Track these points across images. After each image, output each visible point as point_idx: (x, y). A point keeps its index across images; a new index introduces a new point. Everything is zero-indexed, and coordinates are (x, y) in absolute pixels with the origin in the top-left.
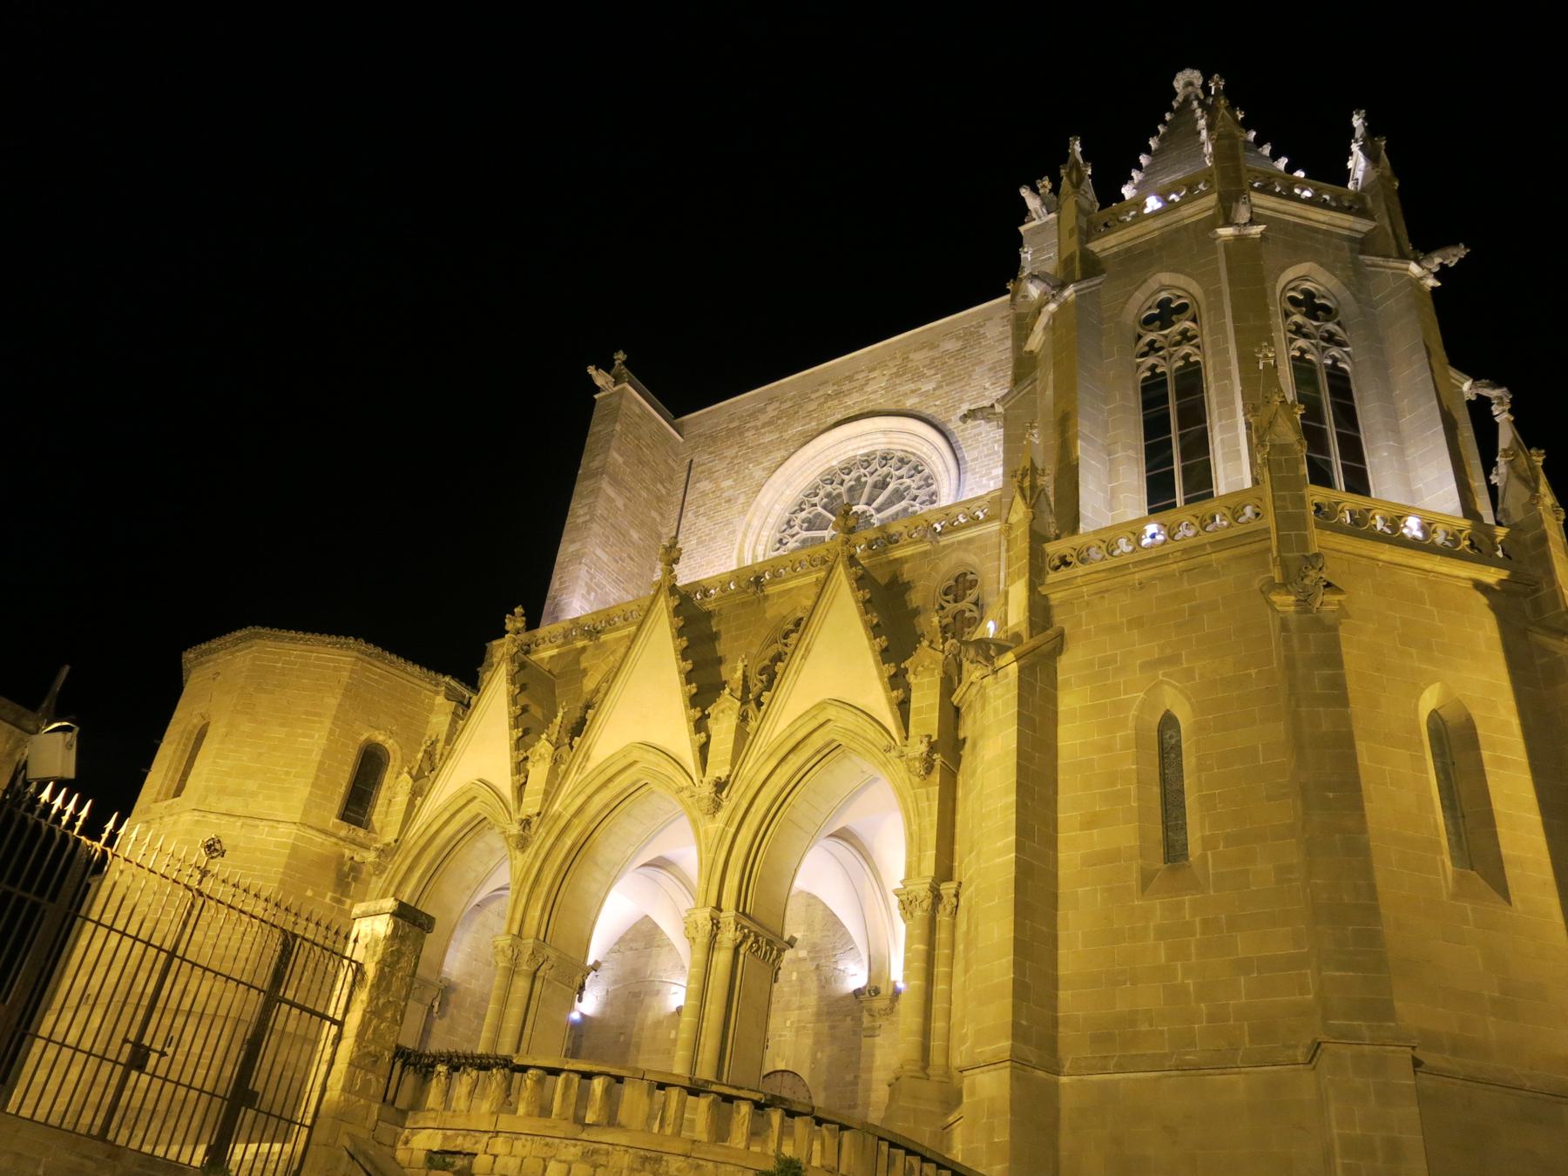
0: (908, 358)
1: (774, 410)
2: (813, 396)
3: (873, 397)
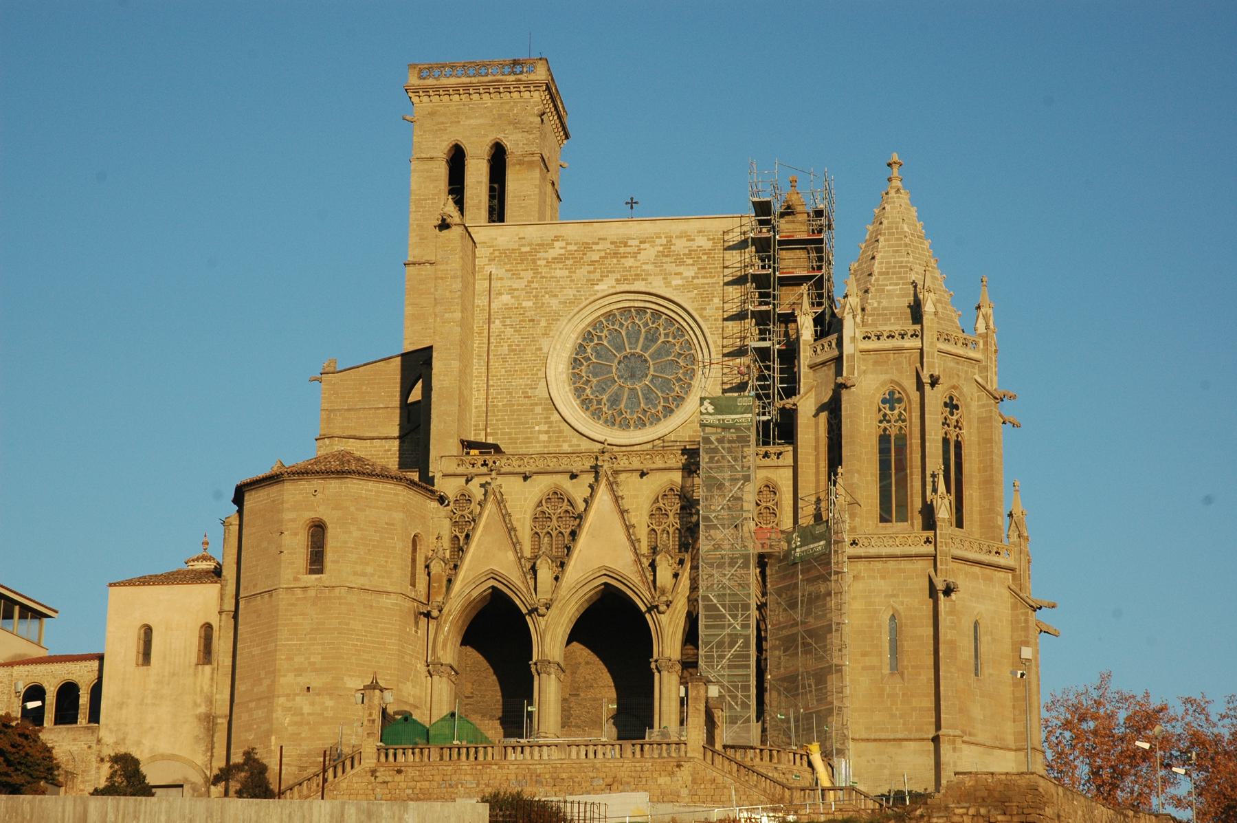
0: (671, 241)
1: (561, 248)
2: (595, 247)
3: (645, 267)
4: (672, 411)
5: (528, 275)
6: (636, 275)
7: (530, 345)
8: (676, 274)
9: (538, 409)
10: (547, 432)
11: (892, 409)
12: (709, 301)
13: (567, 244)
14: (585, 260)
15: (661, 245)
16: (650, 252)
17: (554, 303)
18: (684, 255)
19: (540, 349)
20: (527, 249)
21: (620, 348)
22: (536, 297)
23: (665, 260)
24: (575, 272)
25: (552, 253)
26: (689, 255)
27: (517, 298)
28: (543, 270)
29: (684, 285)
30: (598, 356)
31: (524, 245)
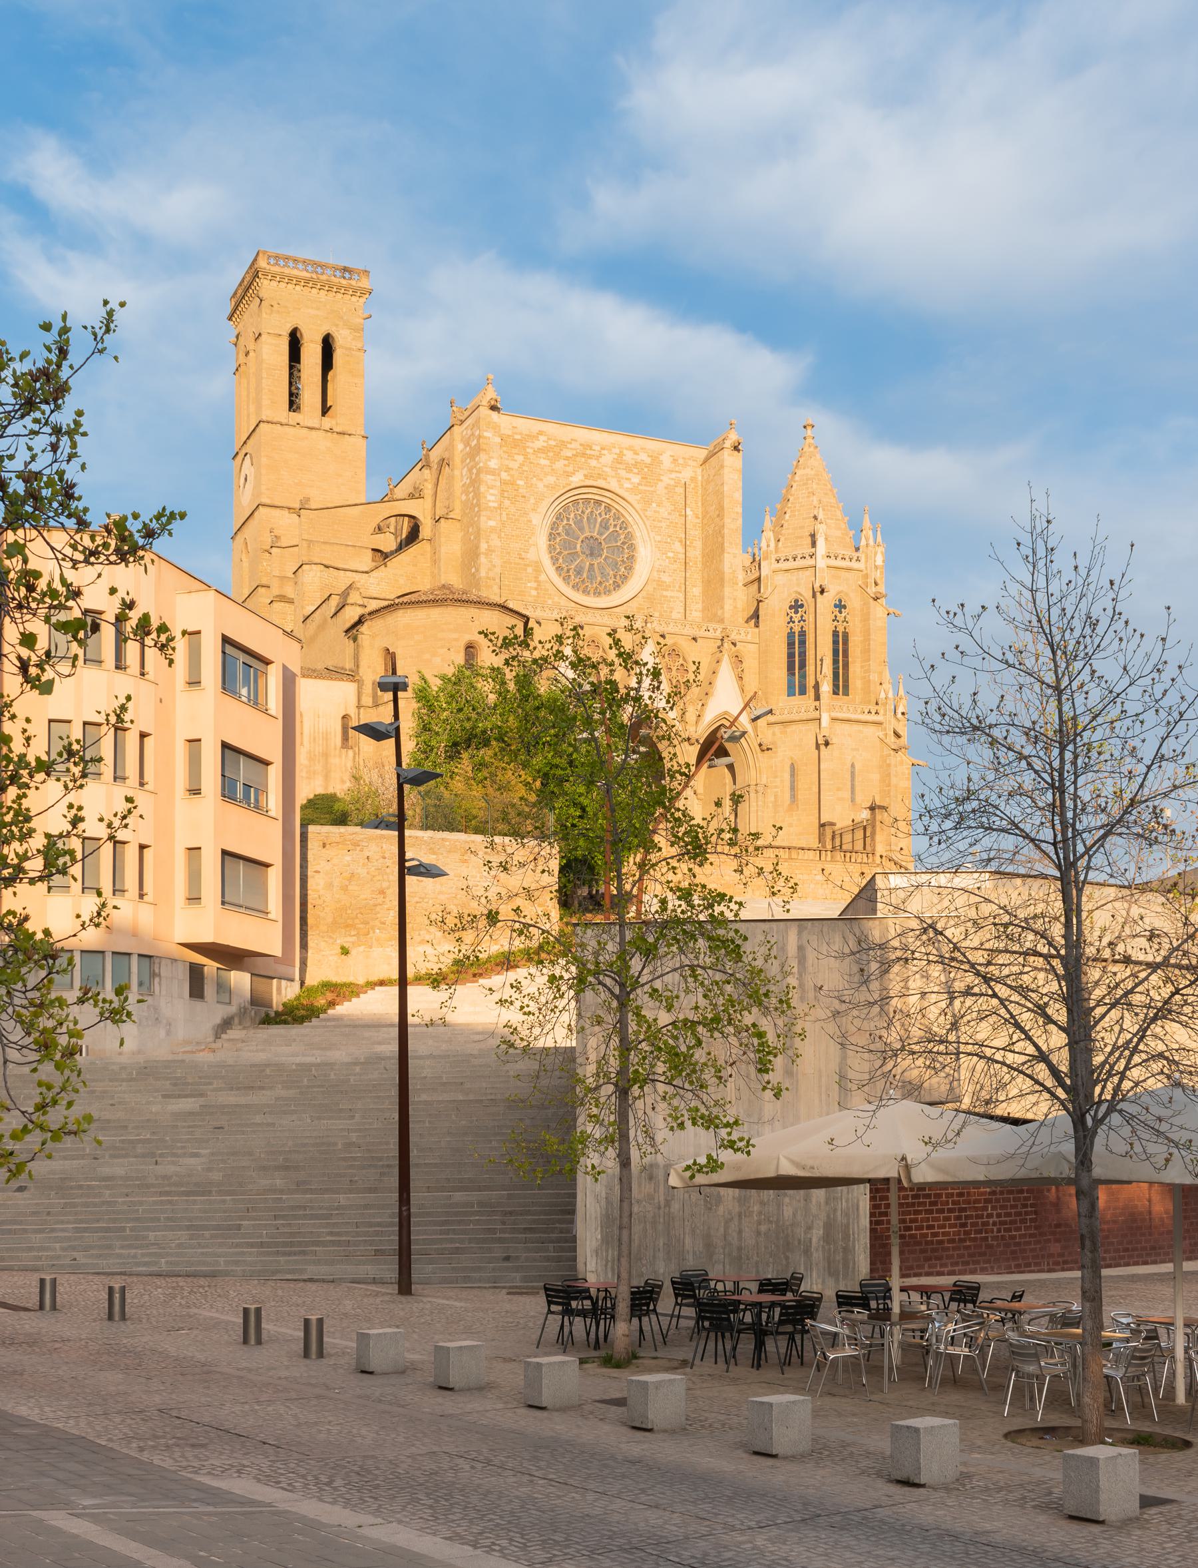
4: (619, 586)
5: (520, 458)
9: (530, 570)
10: (536, 589)
11: (796, 612)
16: (608, 458)
17: (540, 485)
21: (581, 529)
27: (512, 476)
30: (567, 534)
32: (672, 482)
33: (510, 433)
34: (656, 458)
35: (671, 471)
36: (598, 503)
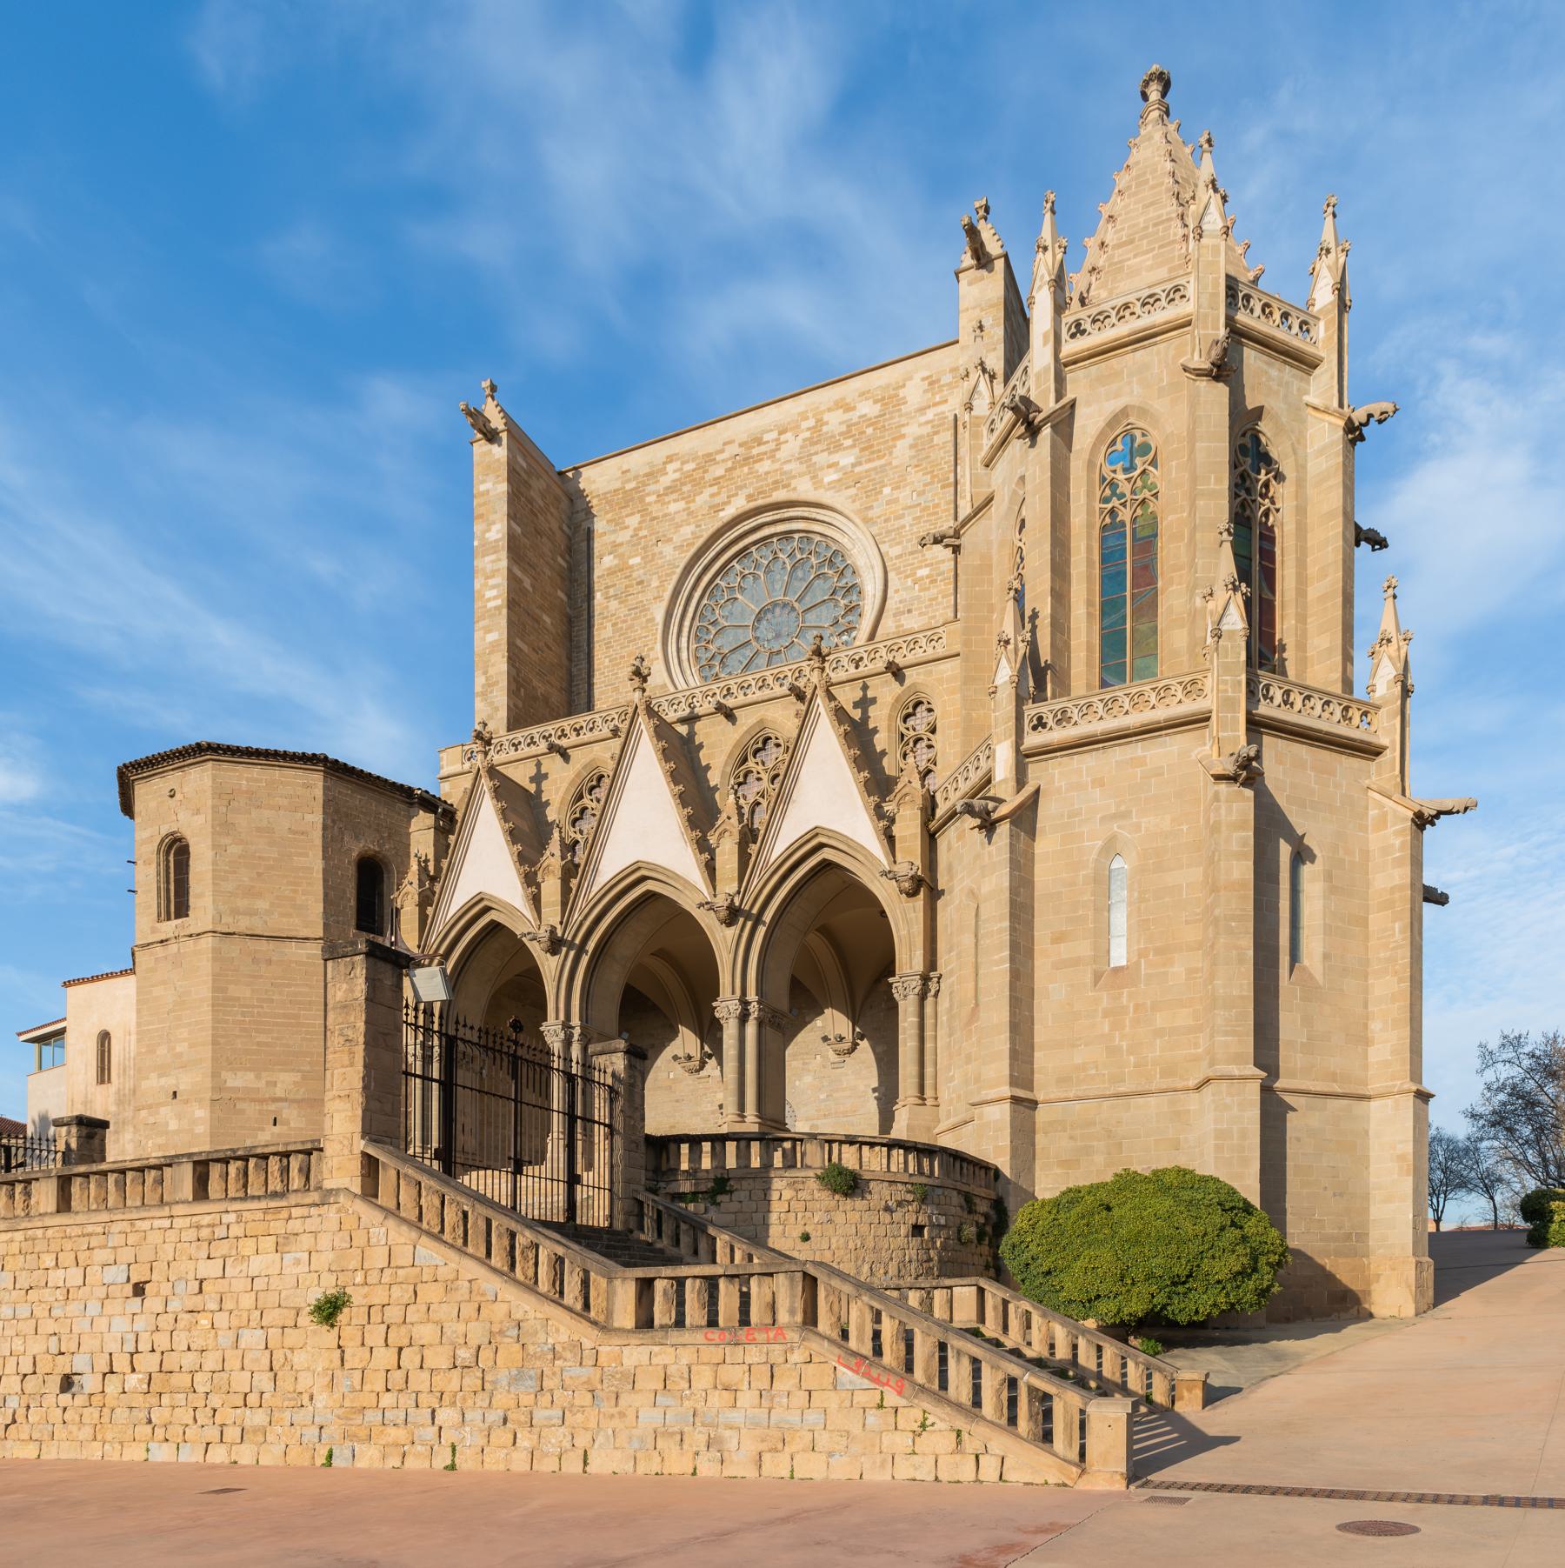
1: (675, 471)
2: (719, 457)
5: (633, 521)
6: (776, 482)
7: (639, 618)
8: (829, 466)
12: (877, 494)
13: (683, 463)
14: (707, 479)
15: (809, 429)
16: (792, 445)
18: (840, 434)
19: (652, 620)
20: (632, 485)
22: (644, 548)
23: (813, 449)
24: (694, 501)
25: (665, 481)
26: (847, 434)
27: (621, 556)
28: (655, 510)
29: (839, 480)
31: (629, 481)
32: (928, 429)
33: (618, 485)
34: (890, 400)
35: (922, 410)
36: (786, 536)
